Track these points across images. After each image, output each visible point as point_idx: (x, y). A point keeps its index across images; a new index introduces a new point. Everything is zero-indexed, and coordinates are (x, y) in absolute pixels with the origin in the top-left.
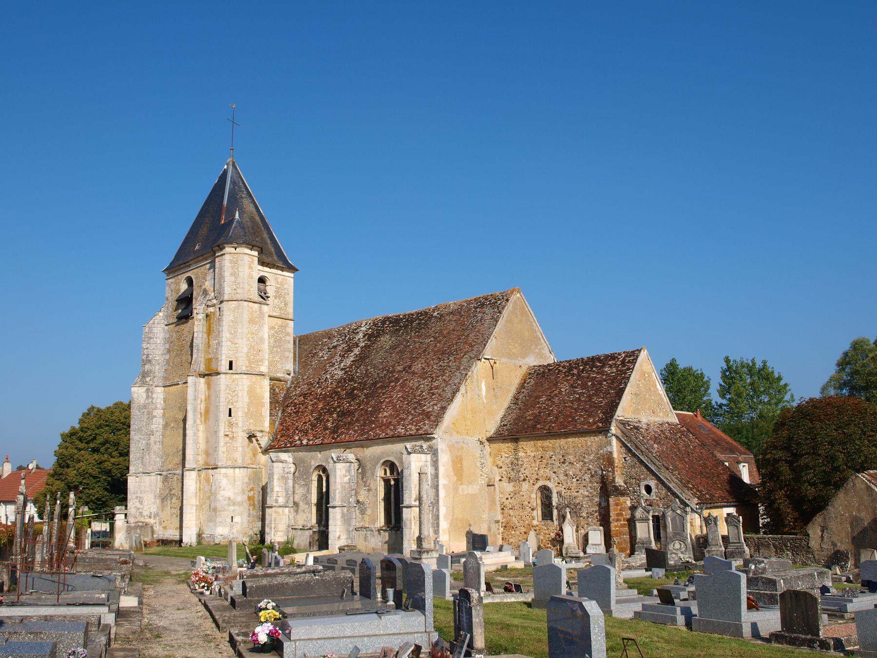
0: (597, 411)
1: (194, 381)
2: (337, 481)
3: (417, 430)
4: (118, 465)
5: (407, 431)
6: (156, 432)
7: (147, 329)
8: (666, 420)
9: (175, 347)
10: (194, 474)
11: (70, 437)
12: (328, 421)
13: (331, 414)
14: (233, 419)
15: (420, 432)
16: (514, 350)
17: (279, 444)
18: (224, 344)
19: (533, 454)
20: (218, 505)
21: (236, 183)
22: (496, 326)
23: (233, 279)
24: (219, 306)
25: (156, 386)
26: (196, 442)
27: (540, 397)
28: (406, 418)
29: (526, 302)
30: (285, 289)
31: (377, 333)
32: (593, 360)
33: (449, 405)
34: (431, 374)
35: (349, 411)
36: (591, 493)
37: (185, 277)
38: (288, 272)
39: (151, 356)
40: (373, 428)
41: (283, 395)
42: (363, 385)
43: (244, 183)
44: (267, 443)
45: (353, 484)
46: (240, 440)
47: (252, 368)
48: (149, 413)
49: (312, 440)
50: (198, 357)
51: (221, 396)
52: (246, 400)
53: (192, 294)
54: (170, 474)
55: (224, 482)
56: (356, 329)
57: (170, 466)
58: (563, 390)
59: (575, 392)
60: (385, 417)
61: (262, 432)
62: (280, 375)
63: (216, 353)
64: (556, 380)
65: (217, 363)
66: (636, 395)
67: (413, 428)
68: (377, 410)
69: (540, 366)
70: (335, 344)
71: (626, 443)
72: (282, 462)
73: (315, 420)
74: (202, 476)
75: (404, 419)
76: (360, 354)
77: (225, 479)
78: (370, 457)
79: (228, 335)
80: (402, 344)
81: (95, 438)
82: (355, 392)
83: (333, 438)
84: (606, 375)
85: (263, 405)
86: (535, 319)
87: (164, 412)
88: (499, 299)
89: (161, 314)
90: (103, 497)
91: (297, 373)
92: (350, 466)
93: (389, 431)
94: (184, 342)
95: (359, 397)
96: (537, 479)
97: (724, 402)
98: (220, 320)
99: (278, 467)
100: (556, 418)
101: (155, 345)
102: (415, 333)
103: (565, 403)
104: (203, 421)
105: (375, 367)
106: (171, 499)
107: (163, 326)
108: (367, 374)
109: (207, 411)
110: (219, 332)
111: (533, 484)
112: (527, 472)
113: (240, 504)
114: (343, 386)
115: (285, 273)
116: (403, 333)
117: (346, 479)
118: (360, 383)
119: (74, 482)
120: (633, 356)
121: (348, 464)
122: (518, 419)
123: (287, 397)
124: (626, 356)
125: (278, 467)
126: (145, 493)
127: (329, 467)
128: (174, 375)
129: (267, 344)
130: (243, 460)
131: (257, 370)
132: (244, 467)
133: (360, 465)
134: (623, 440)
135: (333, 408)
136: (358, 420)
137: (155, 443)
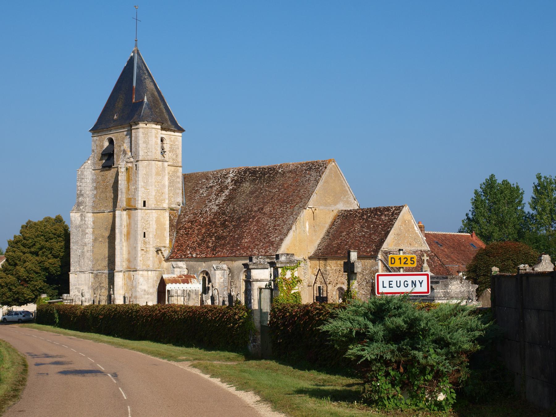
0: (373, 245)
1: (120, 213)
2: (216, 282)
3: (266, 252)
4: (54, 264)
5: (260, 253)
6: (88, 244)
7: (80, 172)
8: (420, 248)
9: (101, 186)
10: (121, 274)
11: (14, 244)
12: (209, 242)
13: (211, 237)
14: (146, 239)
15: (267, 254)
16: (328, 201)
17: (176, 256)
18: (140, 189)
19: (335, 268)
20: (138, 294)
21: (140, 68)
22: (317, 186)
23: (145, 145)
24: (136, 163)
25: (87, 213)
26: (122, 254)
27: (342, 232)
28: (259, 244)
29: (339, 167)
30: (176, 145)
31: (241, 180)
32: (377, 210)
33: (285, 238)
34: (276, 216)
35: (222, 236)
36: (366, 293)
37: (109, 137)
38: (178, 132)
39: (83, 192)
40: (239, 249)
41: (176, 221)
42: (232, 219)
43: (144, 64)
44: (168, 255)
45: (226, 283)
46: (151, 253)
47: (158, 205)
48: (83, 231)
49: (199, 254)
50: (121, 197)
51: (139, 224)
52: (155, 226)
53: (113, 151)
54: (100, 273)
55: (141, 280)
56: (226, 175)
57: (99, 268)
58: (356, 229)
59: (363, 231)
60: (246, 242)
61: (165, 247)
62: (173, 206)
63: (134, 195)
64: (353, 222)
65: (135, 202)
66: (398, 235)
67: (263, 251)
68: (241, 237)
69: (345, 211)
70: (211, 185)
71: (386, 264)
72: (180, 268)
73: (200, 240)
74: (126, 275)
75: (258, 245)
76: (229, 195)
77: (142, 278)
78: (237, 267)
79: (142, 184)
80: (257, 191)
81: (34, 245)
82: (227, 223)
83: (213, 254)
84: (382, 221)
85: (165, 229)
86: (345, 178)
87: (93, 231)
88: (321, 165)
89: (89, 162)
90: (44, 287)
91: (185, 204)
92: (224, 272)
93: (248, 252)
94: (107, 183)
95: (229, 227)
96: (337, 283)
97: (534, 212)
98: (136, 173)
99: (177, 271)
100: (350, 247)
101: (85, 184)
102: (266, 184)
103: (356, 238)
104: (126, 239)
105: (239, 206)
106: (101, 290)
107: (91, 170)
108: (234, 211)
109: (128, 234)
110: (136, 181)
111: (335, 286)
112: (331, 279)
113: (151, 294)
114: (218, 218)
115: (176, 134)
116: (258, 182)
117: (222, 280)
118: (230, 216)
119: (24, 276)
120: (399, 209)
121: (223, 271)
122: (328, 245)
123: (179, 222)
124: (395, 210)
125: (177, 271)
126: (81, 285)
127: (211, 272)
128: (101, 205)
129: (167, 189)
130: (153, 266)
131: (161, 206)
132: (154, 270)
133: (230, 272)
134: (385, 263)
135: (212, 233)
136: (229, 243)
137: (88, 251)
